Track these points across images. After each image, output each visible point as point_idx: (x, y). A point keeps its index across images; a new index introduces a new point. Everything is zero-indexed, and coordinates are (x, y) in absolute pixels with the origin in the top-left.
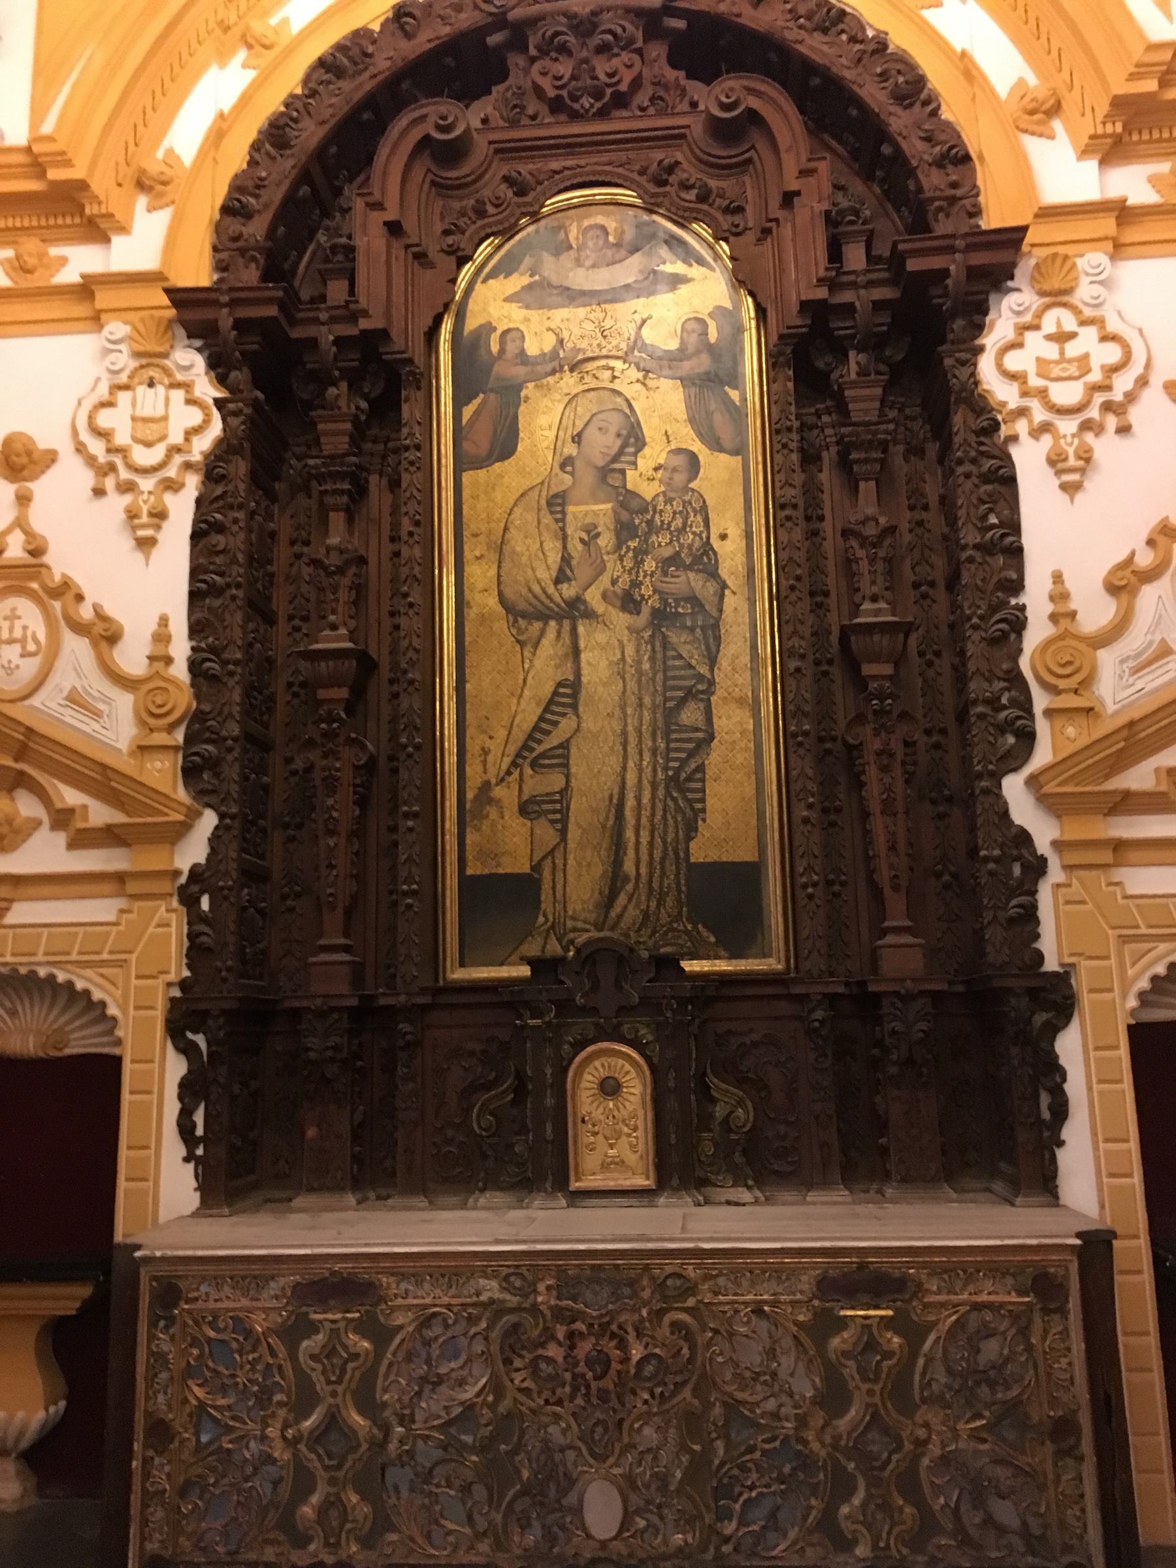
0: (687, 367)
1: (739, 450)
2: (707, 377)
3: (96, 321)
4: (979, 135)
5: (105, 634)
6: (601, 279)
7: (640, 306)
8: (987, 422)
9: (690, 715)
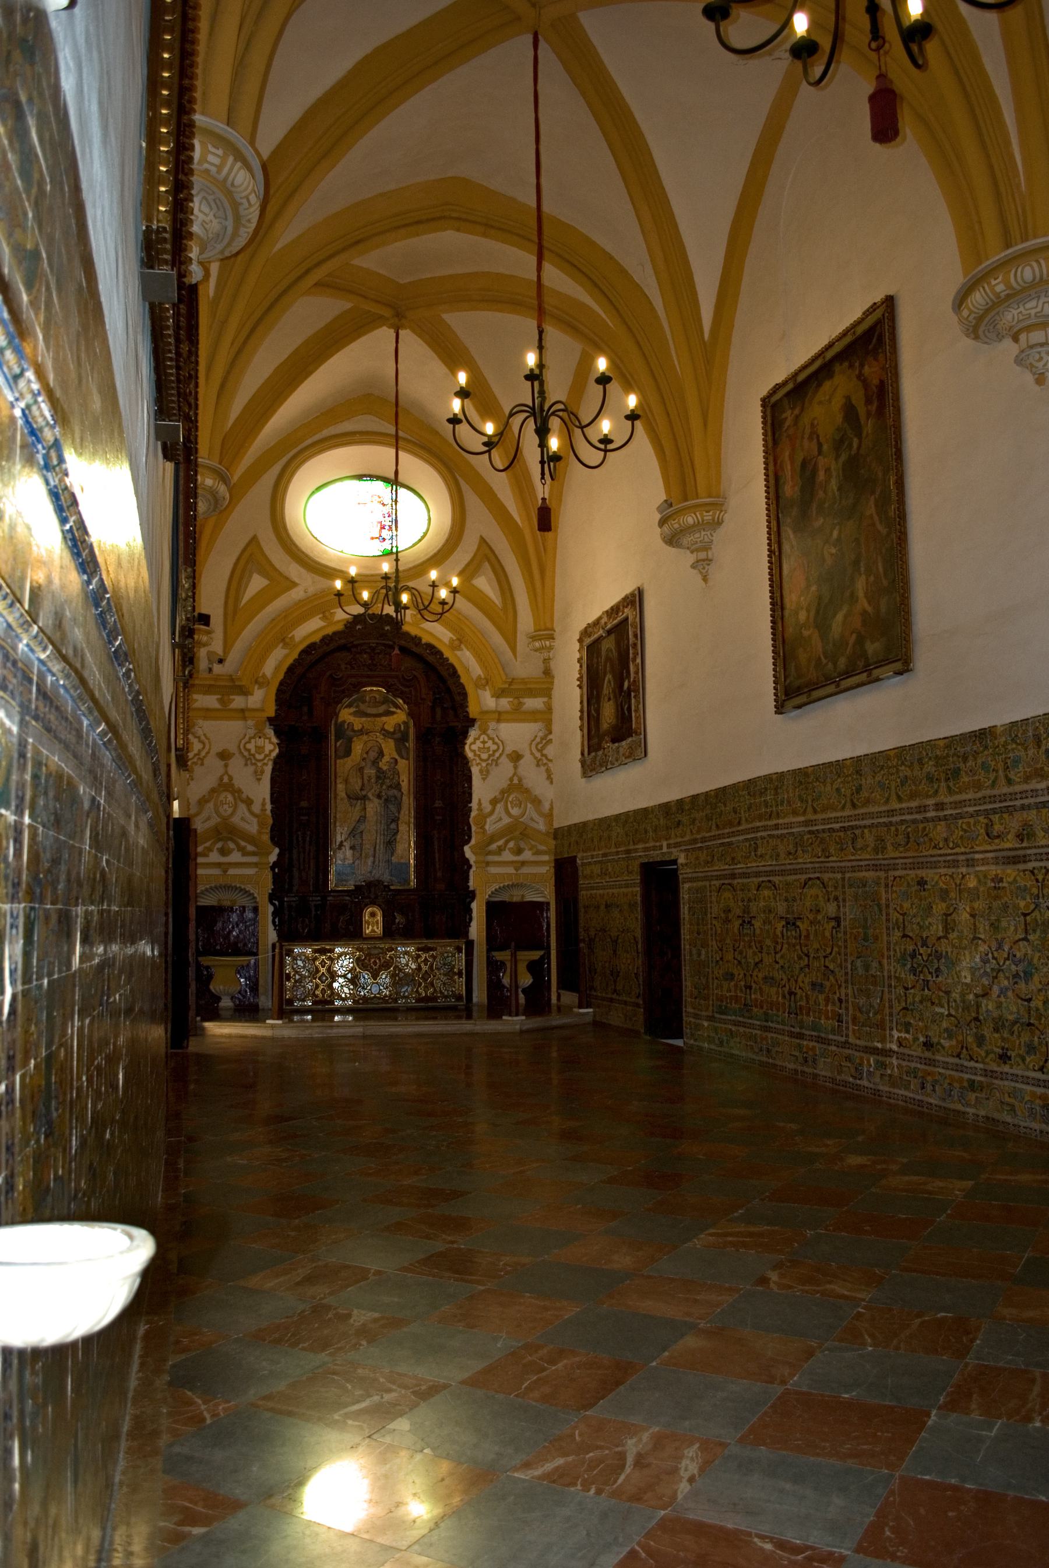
0: (396, 736)
1: (408, 759)
2: (401, 739)
3: (245, 719)
4: (470, 689)
5: (249, 802)
6: (374, 711)
7: (384, 719)
8: (465, 762)
9: (393, 826)
